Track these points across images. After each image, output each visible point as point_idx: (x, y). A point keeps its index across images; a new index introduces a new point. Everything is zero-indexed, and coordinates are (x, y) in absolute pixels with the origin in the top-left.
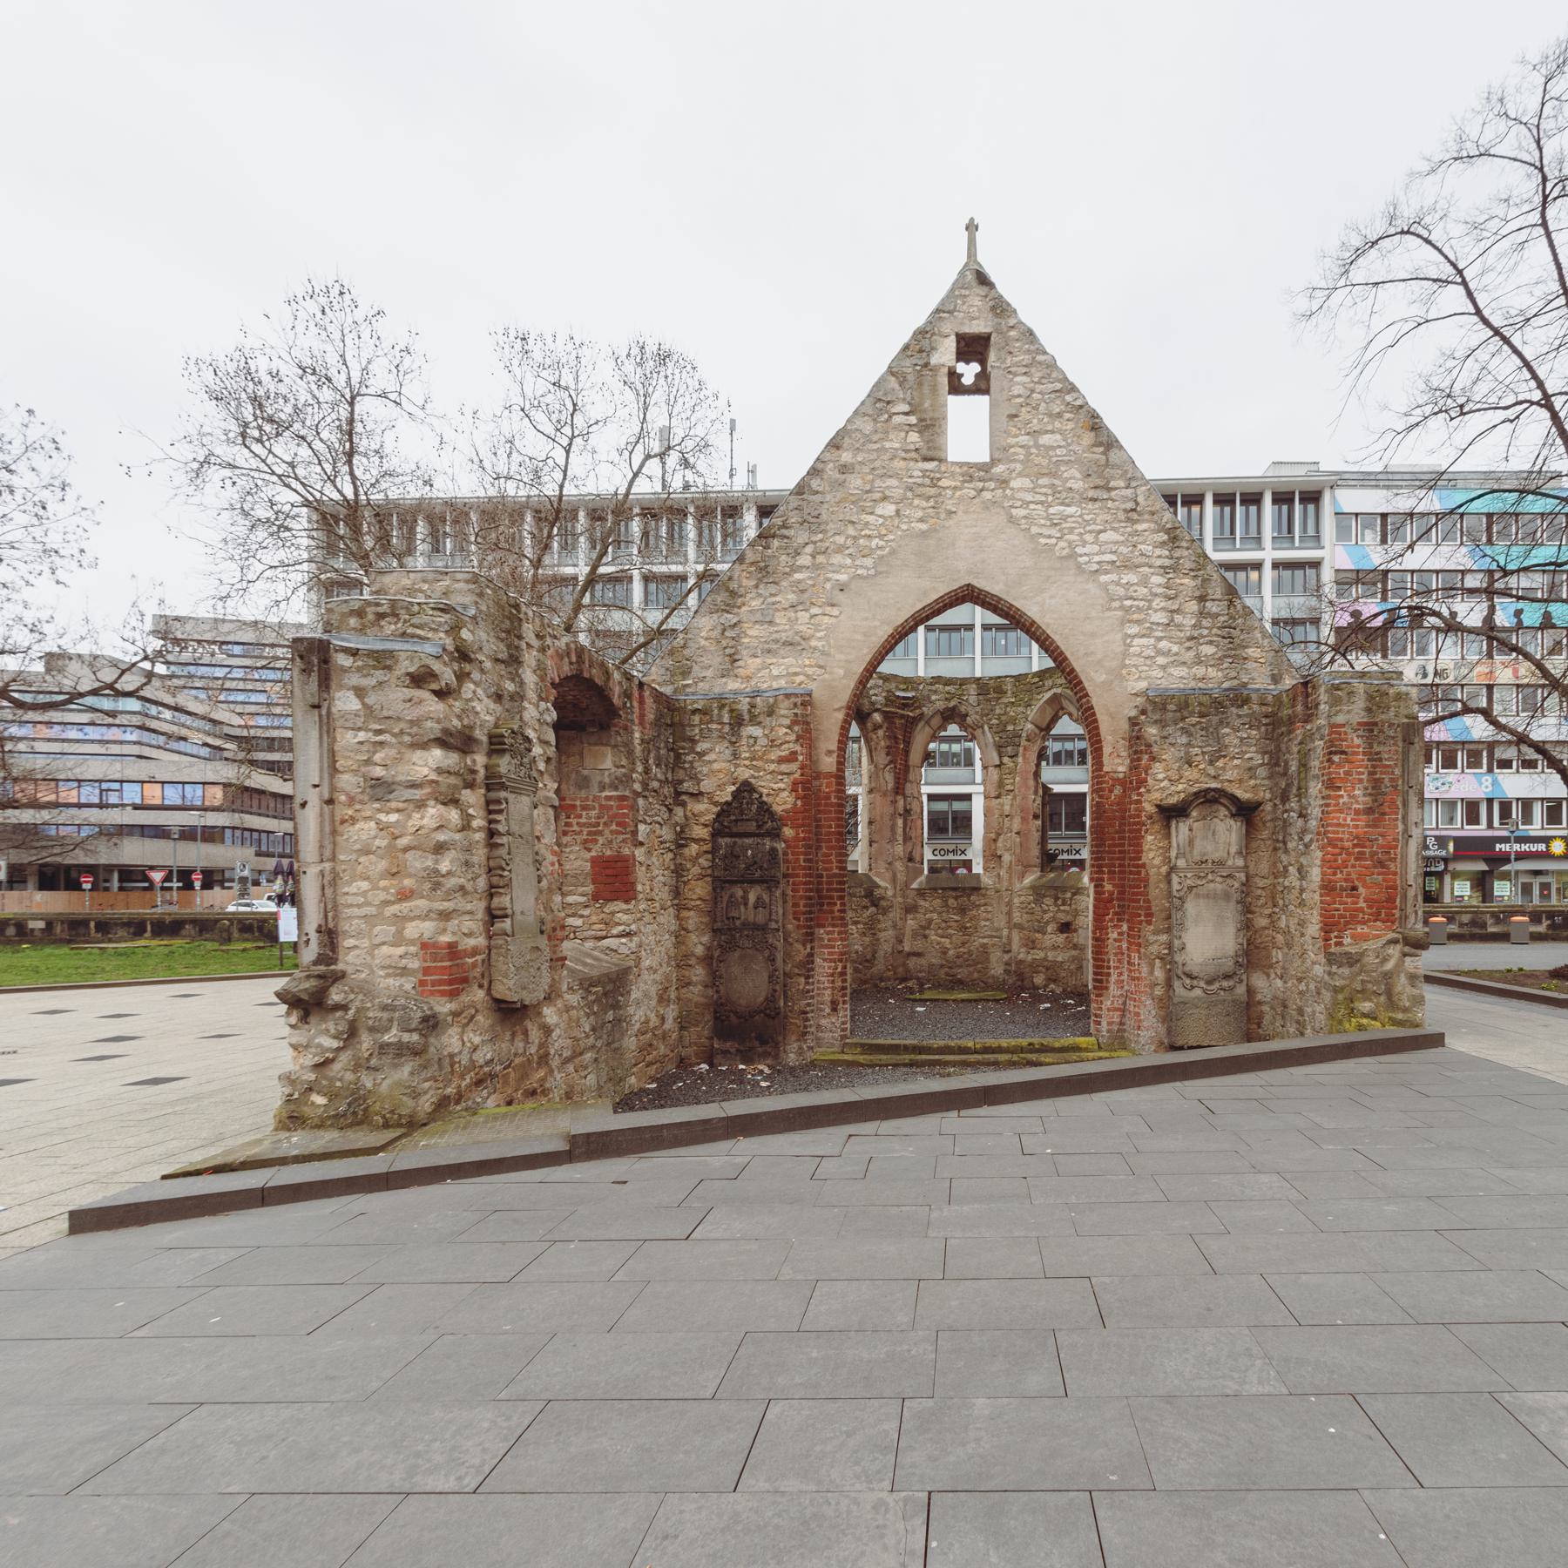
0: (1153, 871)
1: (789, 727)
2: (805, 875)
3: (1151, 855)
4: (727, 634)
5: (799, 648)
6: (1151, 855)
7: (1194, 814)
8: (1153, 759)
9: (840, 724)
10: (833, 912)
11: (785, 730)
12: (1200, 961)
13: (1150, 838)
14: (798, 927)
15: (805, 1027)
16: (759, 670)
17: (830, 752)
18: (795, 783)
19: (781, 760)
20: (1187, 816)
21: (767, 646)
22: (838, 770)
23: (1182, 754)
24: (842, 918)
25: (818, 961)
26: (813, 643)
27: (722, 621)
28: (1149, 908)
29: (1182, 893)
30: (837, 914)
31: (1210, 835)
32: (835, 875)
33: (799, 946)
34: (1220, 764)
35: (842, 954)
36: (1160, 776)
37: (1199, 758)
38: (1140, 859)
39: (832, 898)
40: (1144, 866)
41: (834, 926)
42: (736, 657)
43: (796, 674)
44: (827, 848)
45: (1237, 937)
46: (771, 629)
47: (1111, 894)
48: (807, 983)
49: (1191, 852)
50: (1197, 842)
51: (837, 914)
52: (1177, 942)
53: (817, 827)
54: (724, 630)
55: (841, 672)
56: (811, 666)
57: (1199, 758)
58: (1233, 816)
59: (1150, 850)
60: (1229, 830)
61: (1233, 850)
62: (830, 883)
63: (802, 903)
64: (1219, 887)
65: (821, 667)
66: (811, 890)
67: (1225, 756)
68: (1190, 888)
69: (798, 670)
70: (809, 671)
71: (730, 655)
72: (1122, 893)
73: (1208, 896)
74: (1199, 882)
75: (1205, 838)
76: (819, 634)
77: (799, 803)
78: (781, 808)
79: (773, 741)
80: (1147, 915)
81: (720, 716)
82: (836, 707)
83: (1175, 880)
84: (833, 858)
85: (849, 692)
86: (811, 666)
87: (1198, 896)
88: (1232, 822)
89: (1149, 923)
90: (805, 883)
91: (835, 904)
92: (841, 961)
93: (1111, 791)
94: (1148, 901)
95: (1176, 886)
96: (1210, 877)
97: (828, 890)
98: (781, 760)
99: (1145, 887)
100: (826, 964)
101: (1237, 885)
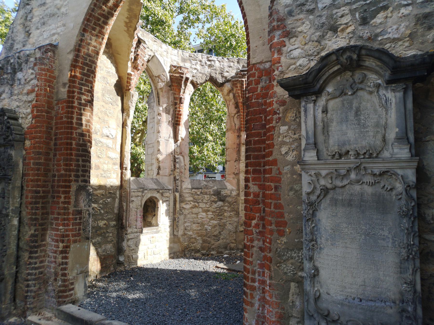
0: (287, 169)
1: (33, 69)
2: (33, 175)
3: (284, 150)
4: (28, 19)
5: (56, 16)
6: (284, 150)
7: (330, 89)
8: (289, 34)
9: (70, 62)
10: (58, 203)
11: (31, 71)
12: (340, 298)
13: (283, 129)
14: (27, 212)
15: (27, 292)
16: (39, 37)
17: (64, 85)
18: (34, 107)
19: (28, 94)
20: (319, 93)
21: (42, 21)
22: (69, 97)
23: (323, 19)
24: (68, 209)
25: (48, 239)
26: (63, 10)
27: (26, 11)
28: (282, 215)
29: (313, 198)
30: (61, 205)
31: (351, 116)
32: (62, 175)
33: (27, 228)
34: (379, 19)
35: (63, 236)
36: (296, 53)
37: (344, 20)
38: (271, 154)
39: (59, 192)
40: (274, 163)
41: (59, 214)
42: (30, 32)
43: (54, 34)
44: (59, 154)
45: (402, 270)
46: (44, 8)
47: (256, 195)
48: (30, 258)
49: (326, 141)
50: (334, 127)
51: (61, 205)
52: (307, 265)
53: (56, 139)
54: (27, 17)
55: (72, 25)
56: (60, 26)
57: (344, 20)
58: (389, 82)
59: (283, 143)
60: (385, 106)
61: (392, 135)
62: (59, 181)
63: (30, 195)
64: (369, 190)
65: (64, 25)
66: (38, 186)
67: (385, 8)
68: (326, 191)
69: (54, 31)
70: (59, 30)
71: (28, 32)
72: (264, 195)
73: (349, 203)
74: (339, 183)
75: (344, 120)
76: (65, 4)
77: (34, 121)
78: (27, 126)
79: (26, 80)
80: (278, 224)
81: (7, 69)
82: (68, 51)
83: (305, 179)
84: (62, 162)
85: (75, 37)
86: (60, 26)
87: (335, 202)
88: (390, 95)
89: (281, 234)
90: (32, 181)
91: (60, 197)
92: (63, 242)
93: (257, 83)
94: (278, 206)
95: (306, 189)
96: (353, 176)
97: (58, 186)
98: (28, 94)
99: (276, 188)
100: (53, 243)
101: (399, 187)
